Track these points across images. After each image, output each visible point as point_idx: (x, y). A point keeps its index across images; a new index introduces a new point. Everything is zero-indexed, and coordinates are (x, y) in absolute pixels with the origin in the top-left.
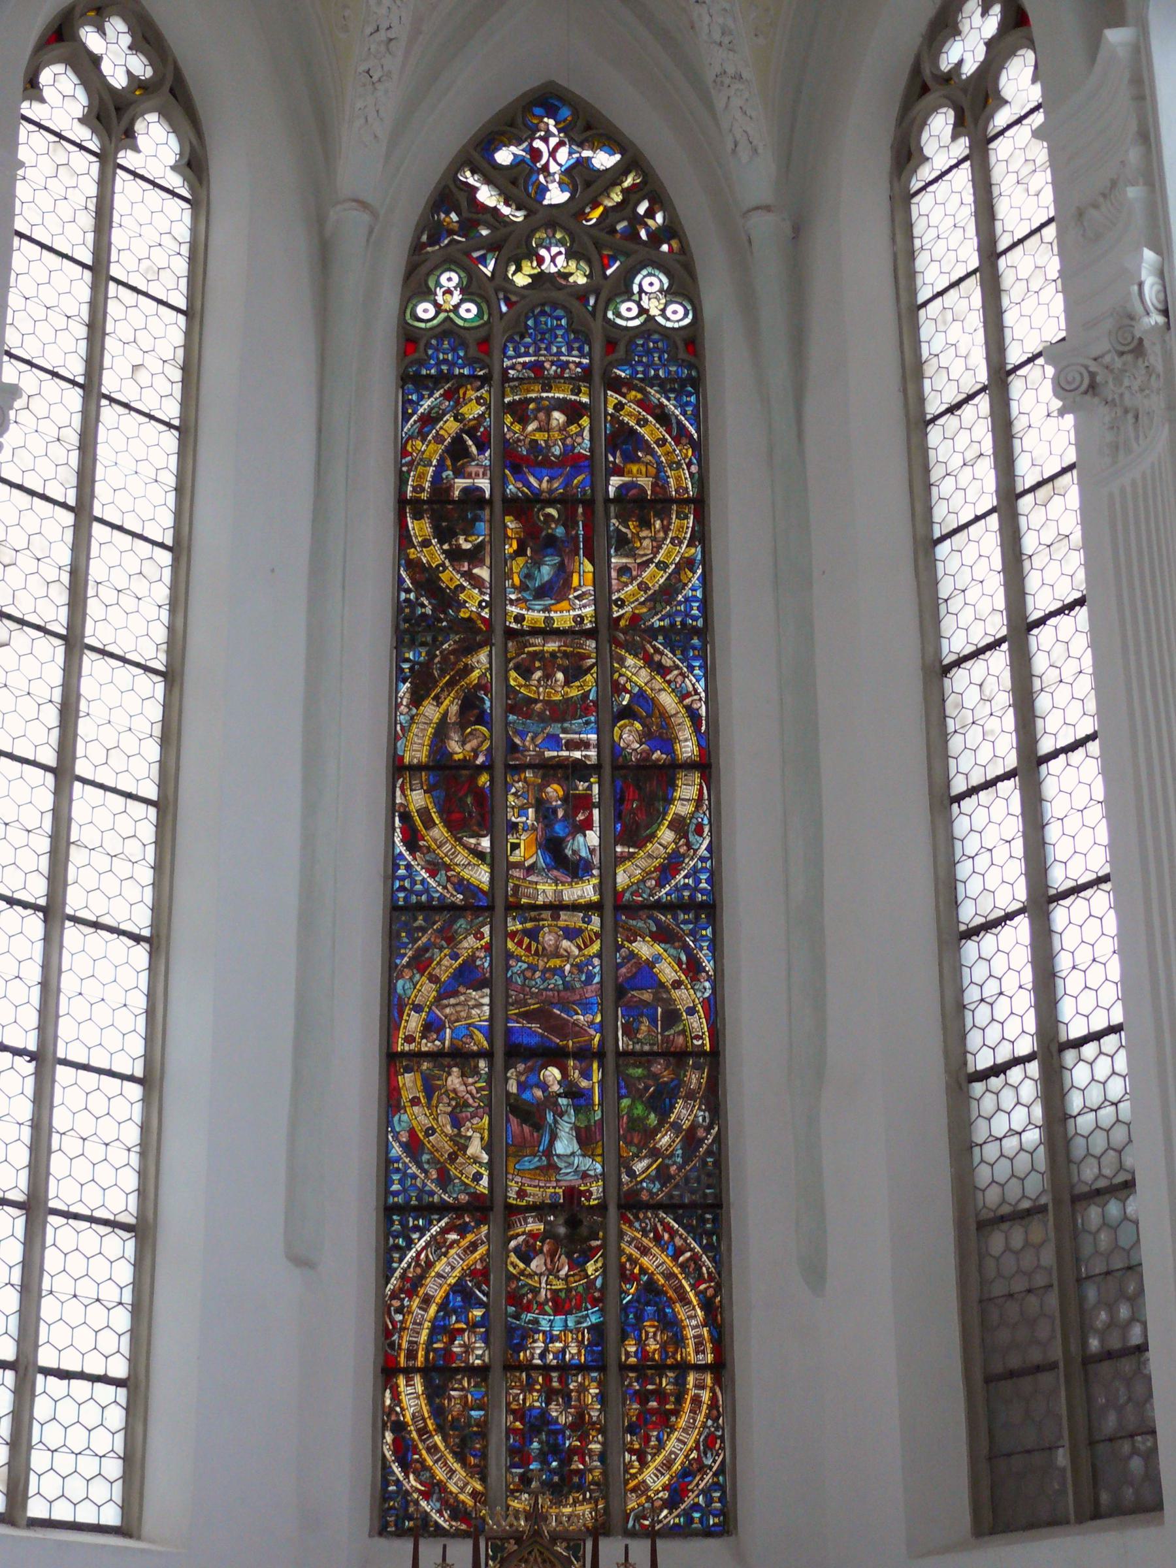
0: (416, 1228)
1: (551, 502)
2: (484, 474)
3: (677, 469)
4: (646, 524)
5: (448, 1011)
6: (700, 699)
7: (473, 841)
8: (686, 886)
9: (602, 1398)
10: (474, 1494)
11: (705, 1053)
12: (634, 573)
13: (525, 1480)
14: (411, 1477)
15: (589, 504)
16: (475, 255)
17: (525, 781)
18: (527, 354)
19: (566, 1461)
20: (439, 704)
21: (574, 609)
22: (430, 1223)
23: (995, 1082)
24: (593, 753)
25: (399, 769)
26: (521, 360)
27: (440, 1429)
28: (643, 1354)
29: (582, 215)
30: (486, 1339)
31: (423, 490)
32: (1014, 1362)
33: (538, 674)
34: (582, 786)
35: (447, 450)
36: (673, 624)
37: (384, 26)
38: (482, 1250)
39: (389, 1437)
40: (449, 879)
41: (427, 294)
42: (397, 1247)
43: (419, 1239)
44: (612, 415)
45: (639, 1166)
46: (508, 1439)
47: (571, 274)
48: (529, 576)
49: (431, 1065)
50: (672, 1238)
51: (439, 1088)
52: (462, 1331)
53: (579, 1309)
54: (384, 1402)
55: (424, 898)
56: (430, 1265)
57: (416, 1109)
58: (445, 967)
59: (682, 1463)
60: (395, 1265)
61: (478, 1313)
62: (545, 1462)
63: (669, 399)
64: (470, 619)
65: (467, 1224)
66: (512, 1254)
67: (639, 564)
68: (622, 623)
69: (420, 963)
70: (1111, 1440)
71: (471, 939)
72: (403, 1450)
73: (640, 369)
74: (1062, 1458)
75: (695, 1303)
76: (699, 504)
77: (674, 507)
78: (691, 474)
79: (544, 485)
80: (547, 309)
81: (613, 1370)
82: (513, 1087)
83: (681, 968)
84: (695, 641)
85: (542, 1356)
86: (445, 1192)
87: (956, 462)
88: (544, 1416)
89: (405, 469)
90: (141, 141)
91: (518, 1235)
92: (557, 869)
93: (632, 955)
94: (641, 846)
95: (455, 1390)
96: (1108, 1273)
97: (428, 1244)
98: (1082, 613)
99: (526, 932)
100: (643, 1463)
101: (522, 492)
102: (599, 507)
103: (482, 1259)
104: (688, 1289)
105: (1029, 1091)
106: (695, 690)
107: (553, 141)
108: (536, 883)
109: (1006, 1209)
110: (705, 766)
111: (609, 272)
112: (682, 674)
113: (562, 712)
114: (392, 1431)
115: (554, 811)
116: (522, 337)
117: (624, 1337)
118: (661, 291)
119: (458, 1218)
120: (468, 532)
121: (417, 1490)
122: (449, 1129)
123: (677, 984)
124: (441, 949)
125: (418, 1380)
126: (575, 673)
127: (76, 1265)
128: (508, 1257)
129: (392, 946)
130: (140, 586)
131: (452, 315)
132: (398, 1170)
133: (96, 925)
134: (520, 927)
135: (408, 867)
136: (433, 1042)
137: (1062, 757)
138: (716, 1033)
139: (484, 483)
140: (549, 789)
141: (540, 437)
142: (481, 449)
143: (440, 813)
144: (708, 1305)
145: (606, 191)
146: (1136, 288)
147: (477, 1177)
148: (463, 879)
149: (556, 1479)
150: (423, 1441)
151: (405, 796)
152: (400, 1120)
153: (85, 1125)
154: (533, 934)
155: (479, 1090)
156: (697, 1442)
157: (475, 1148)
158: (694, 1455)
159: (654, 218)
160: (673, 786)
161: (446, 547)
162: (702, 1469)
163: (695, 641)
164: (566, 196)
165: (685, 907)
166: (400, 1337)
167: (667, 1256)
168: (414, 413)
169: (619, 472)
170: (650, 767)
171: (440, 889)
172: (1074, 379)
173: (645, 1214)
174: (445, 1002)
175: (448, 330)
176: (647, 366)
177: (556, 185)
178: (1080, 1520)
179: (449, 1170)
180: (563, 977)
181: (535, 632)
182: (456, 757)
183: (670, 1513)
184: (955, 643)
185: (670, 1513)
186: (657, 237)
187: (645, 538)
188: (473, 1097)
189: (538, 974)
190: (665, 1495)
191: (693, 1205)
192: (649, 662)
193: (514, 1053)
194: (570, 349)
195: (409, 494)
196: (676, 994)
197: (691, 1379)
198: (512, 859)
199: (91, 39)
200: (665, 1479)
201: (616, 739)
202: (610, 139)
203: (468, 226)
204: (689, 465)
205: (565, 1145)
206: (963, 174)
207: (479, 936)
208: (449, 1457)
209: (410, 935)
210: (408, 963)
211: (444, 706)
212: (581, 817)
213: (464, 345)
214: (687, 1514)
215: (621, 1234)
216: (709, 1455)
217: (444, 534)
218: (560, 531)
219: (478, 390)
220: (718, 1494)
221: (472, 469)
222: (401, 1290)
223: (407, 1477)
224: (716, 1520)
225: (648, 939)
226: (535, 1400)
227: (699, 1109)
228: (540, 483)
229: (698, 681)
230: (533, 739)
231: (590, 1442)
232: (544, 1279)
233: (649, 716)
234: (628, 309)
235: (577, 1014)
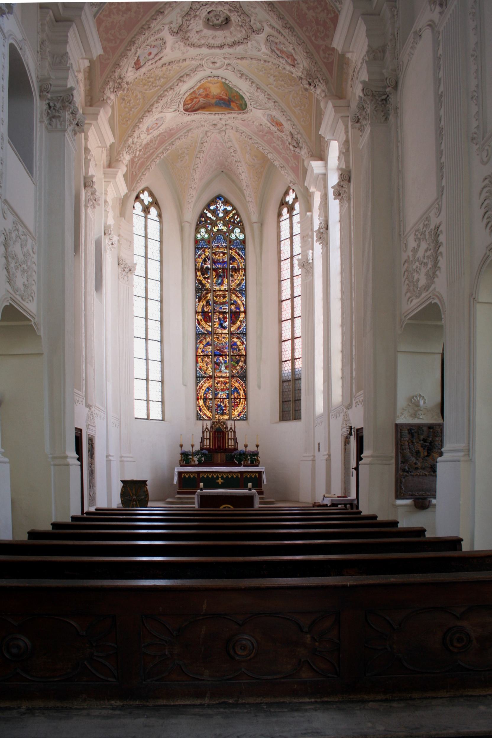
4: (236, 273)
9: (229, 403)
13: (218, 413)
15: (227, 269)
24: (227, 310)
25: (196, 312)
27: (205, 407)
28: (234, 397)
30: (212, 395)
34: (225, 315)
35: (203, 260)
38: (211, 383)
39: (198, 408)
41: (199, 232)
48: (217, 282)
58: (204, 342)
69: (201, 342)
72: (200, 410)
76: (245, 269)
82: (215, 360)
84: (244, 292)
88: (220, 405)
93: (233, 341)
99: (217, 338)
102: (228, 270)
107: (220, 205)
110: (245, 312)
113: (223, 303)
117: (232, 394)
120: (207, 274)
123: (240, 345)
125: (202, 400)
126: (224, 297)
129: (196, 340)
138: (246, 352)
139: (209, 266)
141: (219, 258)
142: (209, 260)
143: (203, 319)
144: (244, 390)
145: (229, 214)
147: (210, 373)
154: (218, 338)
157: (210, 369)
160: (240, 315)
162: (243, 412)
165: (242, 333)
175: (203, 239)
176: (236, 246)
181: (218, 291)
186: (238, 223)
191: (242, 377)
193: (215, 355)
194: (223, 243)
196: (240, 347)
197: (241, 400)
200: (238, 413)
202: (231, 205)
203: (206, 221)
205: (223, 368)
207: (210, 338)
213: (206, 242)
214: (241, 418)
215: (231, 381)
217: (203, 275)
218: (222, 274)
221: (207, 263)
226: (219, 403)
228: (219, 266)
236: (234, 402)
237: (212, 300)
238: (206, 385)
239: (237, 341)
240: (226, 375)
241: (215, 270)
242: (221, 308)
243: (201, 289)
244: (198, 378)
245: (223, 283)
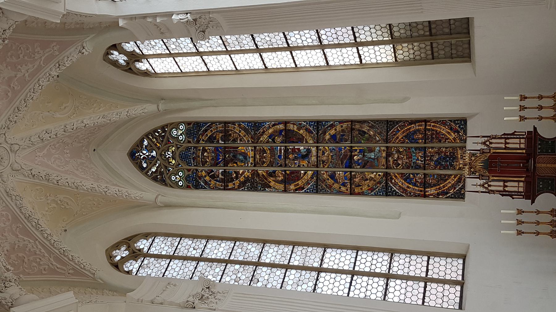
0: (391, 189)
1: (225, 156)
2: (218, 171)
3: (218, 128)
4: (230, 135)
5: (341, 181)
6: (270, 123)
7: (302, 175)
8: (313, 127)
9: (432, 148)
10: (455, 177)
11: (352, 124)
12: (241, 138)
14: (450, 192)
15: (225, 147)
16: (168, 172)
17: (288, 163)
18: (191, 161)
19: (447, 156)
20: (271, 182)
21: (250, 151)
22: (390, 186)
23: (363, 57)
24: (282, 148)
25: (285, 191)
26: (192, 162)
27: (439, 185)
29: (159, 148)
30: (417, 174)
31: (222, 185)
32: (429, 52)
33: (264, 160)
34: (290, 150)
36: (253, 129)
37: (115, 192)
39: (441, 196)
40: (310, 180)
42: (395, 193)
43: (394, 189)
44: (205, 142)
45: (378, 139)
46: (441, 169)
47: (172, 151)
48: (242, 161)
49: (353, 185)
50: (395, 132)
51: (358, 183)
52: (415, 179)
53: (410, 153)
54: (432, 198)
55: (315, 186)
56: (400, 186)
57: (363, 189)
58: (331, 181)
59: (449, 130)
60: (400, 194)
61: (411, 175)
62: (447, 161)
63: (202, 129)
64: (252, 175)
65: (390, 178)
66: (397, 168)
67: (239, 137)
68: (253, 141)
69: (330, 187)
70: (451, 30)
71: (324, 176)
73: (194, 135)
74: (453, 41)
75: (410, 126)
76: (226, 123)
77: (226, 128)
78: (219, 125)
79: (221, 157)
80: (180, 156)
81: (426, 145)
83: (332, 128)
84: (257, 124)
85: (422, 161)
86: (383, 183)
87: (218, 64)
88: (436, 161)
89: (217, 189)
90: (141, 247)
91: (393, 166)
92: (309, 156)
93: (328, 140)
94: (304, 137)
95: (429, 182)
96: (411, 30)
97: (395, 187)
98: (255, 35)
100: (448, 139)
101: (223, 162)
103: (399, 175)
104: (407, 128)
105: (365, 49)
106: (268, 125)
107: (141, 154)
108: (312, 161)
109: (393, 55)
110: (286, 123)
111: (172, 142)
112: (265, 127)
114: (439, 195)
115: (296, 157)
116: (187, 162)
118: (176, 130)
119: (389, 180)
120: (232, 174)
121: (454, 190)
122: (368, 181)
123: (336, 130)
124: (326, 182)
125: (427, 190)
126: (264, 151)
127: (401, 267)
128: (398, 168)
131: (182, 178)
132: (377, 193)
133: (322, 260)
134: (322, 165)
135: (307, 189)
136: (348, 185)
137: (288, 41)
139: (221, 171)
140: (290, 158)
142: (213, 171)
145: (153, 142)
146: (181, 20)
147: (379, 175)
148: (310, 177)
149: (451, 159)
150: (442, 189)
151: (291, 190)
152: (366, 192)
153: (368, 264)
154: (323, 162)
155: (359, 175)
156: (443, 126)
158: (447, 127)
159: (160, 132)
161: (235, 180)
162: (450, 125)
163: (257, 124)
164: (154, 151)
166: (417, 193)
167: (399, 133)
168: (204, 186)
169: (218, 141)
170: (286, 135)
171: (313, 182)
172: (202, 36)
173: (389, 138)
174: (339, 182)
177: (151, 154)
178: (470, 37)
179: (378, 182)
180: (333, 155)
181: (254, 160)
182: (283, 178)
183: (461, 132)
184: (260, 66)
185: (461, 132)
186: (164, 131)
187: (234, 135)
188: (361, 176)
189: (333, 161)
190: (456, 134)
191: (387, 126)
192: (262, 135)
194: (190, 151)
195: (223, 188)
198: (306, 166)
201: (279, 142)
202: (142, 141)
203: (161, 173)
204: (217, 125)
205: (372, 155)
206: (151, 61)
207: (324, 174)
208: (446, 183)
209: (323, 189)
210: (329, 190)
211: (271, 181)
212: (297, 151)
216: (447, 123)
217: (232, 180)
219: (199, 172)
220: (456, 122)
222: (406, 193)
223: (450, 193)
224: (463, 122)
225: (325, 136)
227: (365, 125)
229: (266, 124)
230: (279, 161)
231: (443, 151)
232: (404, 161)
233: (274, 135)
234: (181, 138)
235: (342, 152)
236: (433, 138)
237: (267, 169)
238: (400, 182)
239: (329, 134)
240: (384, 151)
241: (226, 165)
242: (280, 157)
243: (252, 184)
244: (388, 192)
245: (244, 153)
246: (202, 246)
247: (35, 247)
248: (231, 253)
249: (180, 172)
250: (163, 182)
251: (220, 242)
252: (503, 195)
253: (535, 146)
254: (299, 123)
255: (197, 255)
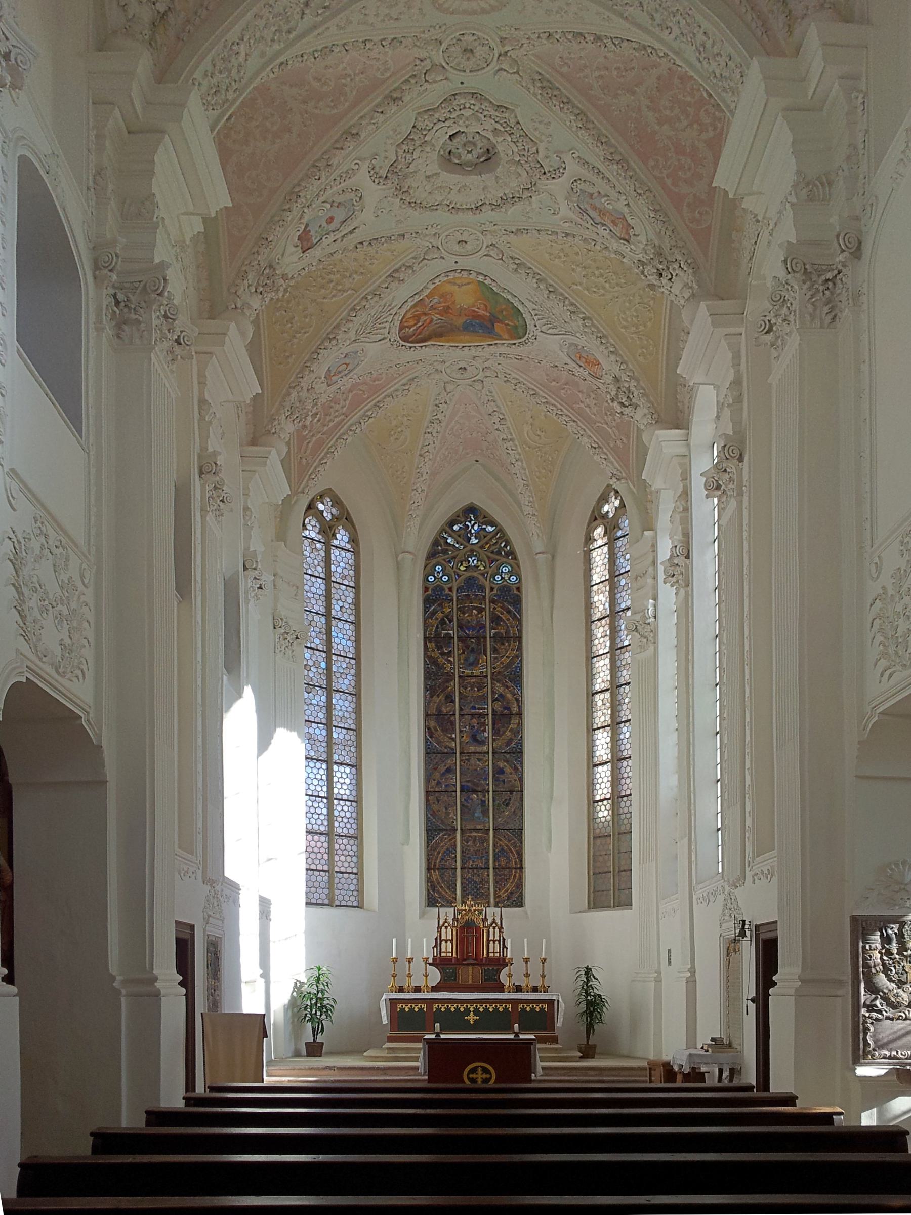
1: (473, 638)
15: (485, 638)
48: (466, 660)
90: (338, 536)
130: (347, 671)
139: (451, 632)
192: (503, 685)
199: (321, 507)
203: (445, 552)
245: (478, 663)
246: (346, 617)
247: (337, 414)
248: (340, 655)
249: (447, 578)
250: (432, 555)
251: (353, 639)
252: (436, 939)
253: (491, 965)
254: (519, 731)
255: (333, 613)
